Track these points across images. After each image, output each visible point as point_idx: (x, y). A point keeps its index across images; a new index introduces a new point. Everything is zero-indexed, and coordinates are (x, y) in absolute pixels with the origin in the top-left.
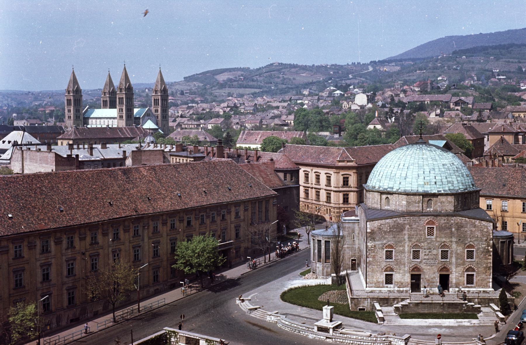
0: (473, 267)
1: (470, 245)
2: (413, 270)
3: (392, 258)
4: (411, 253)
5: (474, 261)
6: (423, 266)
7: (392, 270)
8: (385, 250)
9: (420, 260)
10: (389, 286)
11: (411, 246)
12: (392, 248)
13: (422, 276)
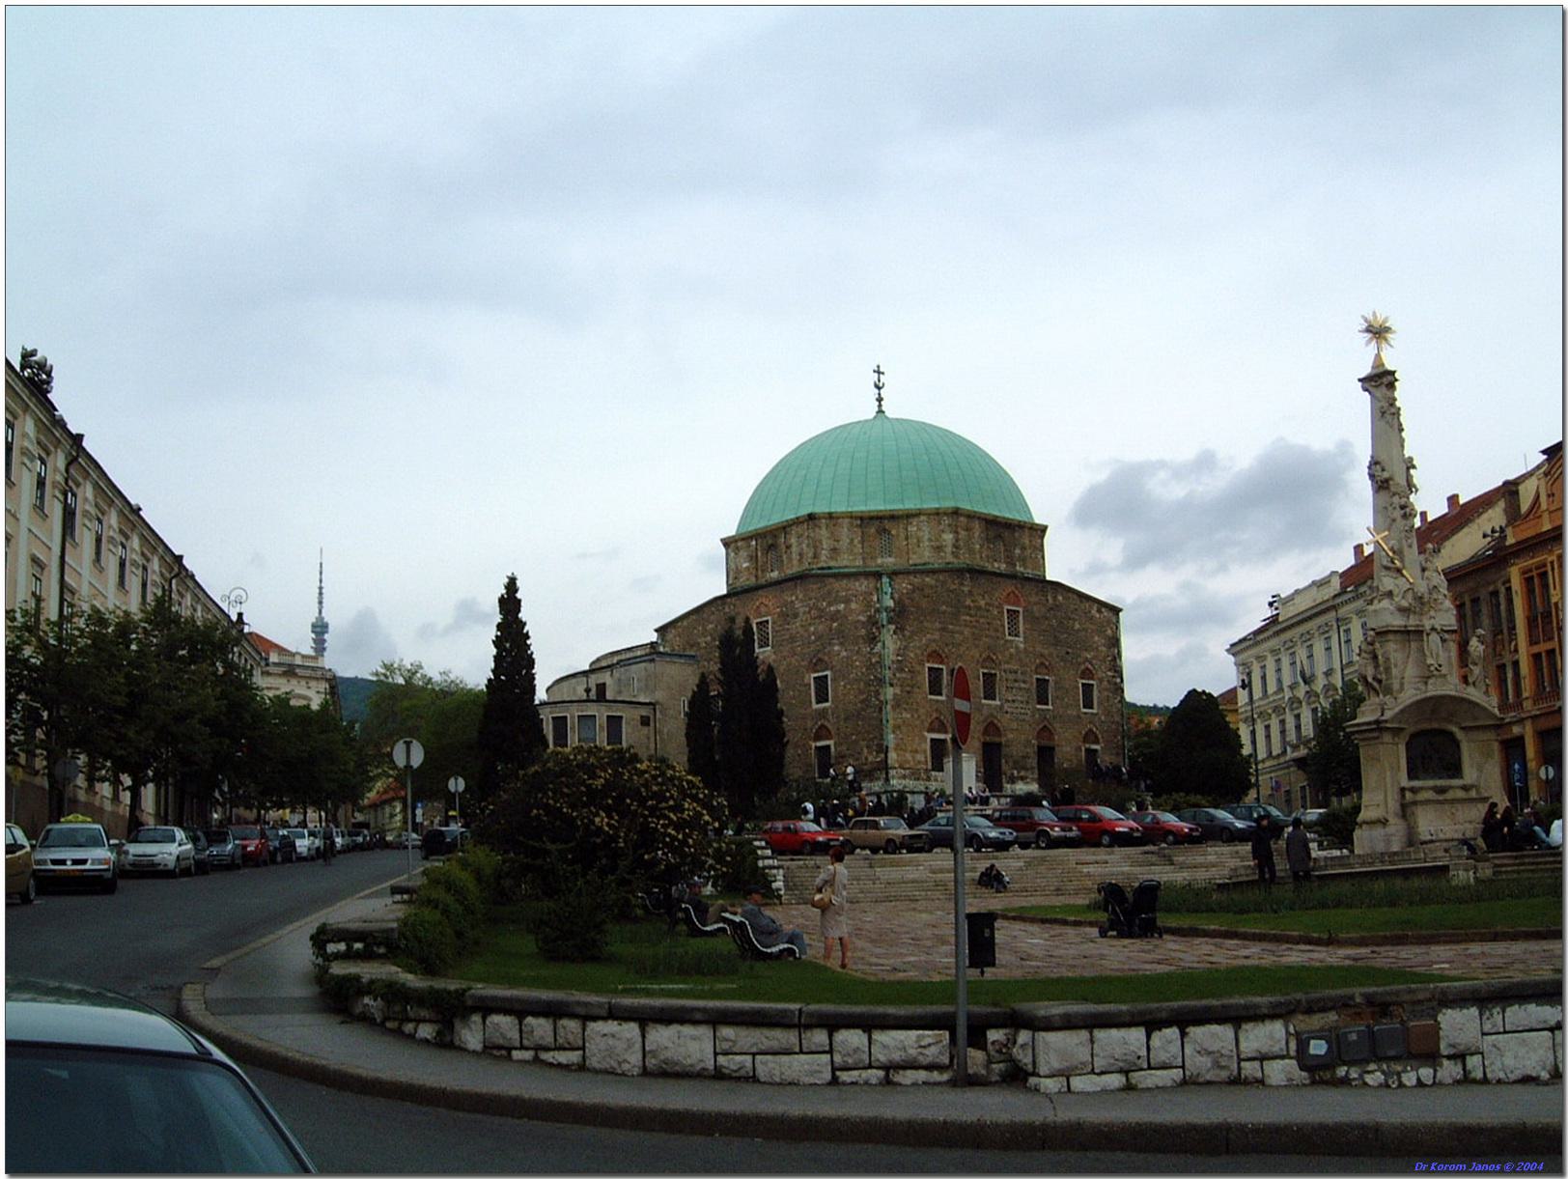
1: (1087, 669)
2: (986, 732)
5: (1097, 714)
6: (1004, 721)
8: (928, 665)
9: (998, 703)
12: (941, 663)
13: (1005, 751)
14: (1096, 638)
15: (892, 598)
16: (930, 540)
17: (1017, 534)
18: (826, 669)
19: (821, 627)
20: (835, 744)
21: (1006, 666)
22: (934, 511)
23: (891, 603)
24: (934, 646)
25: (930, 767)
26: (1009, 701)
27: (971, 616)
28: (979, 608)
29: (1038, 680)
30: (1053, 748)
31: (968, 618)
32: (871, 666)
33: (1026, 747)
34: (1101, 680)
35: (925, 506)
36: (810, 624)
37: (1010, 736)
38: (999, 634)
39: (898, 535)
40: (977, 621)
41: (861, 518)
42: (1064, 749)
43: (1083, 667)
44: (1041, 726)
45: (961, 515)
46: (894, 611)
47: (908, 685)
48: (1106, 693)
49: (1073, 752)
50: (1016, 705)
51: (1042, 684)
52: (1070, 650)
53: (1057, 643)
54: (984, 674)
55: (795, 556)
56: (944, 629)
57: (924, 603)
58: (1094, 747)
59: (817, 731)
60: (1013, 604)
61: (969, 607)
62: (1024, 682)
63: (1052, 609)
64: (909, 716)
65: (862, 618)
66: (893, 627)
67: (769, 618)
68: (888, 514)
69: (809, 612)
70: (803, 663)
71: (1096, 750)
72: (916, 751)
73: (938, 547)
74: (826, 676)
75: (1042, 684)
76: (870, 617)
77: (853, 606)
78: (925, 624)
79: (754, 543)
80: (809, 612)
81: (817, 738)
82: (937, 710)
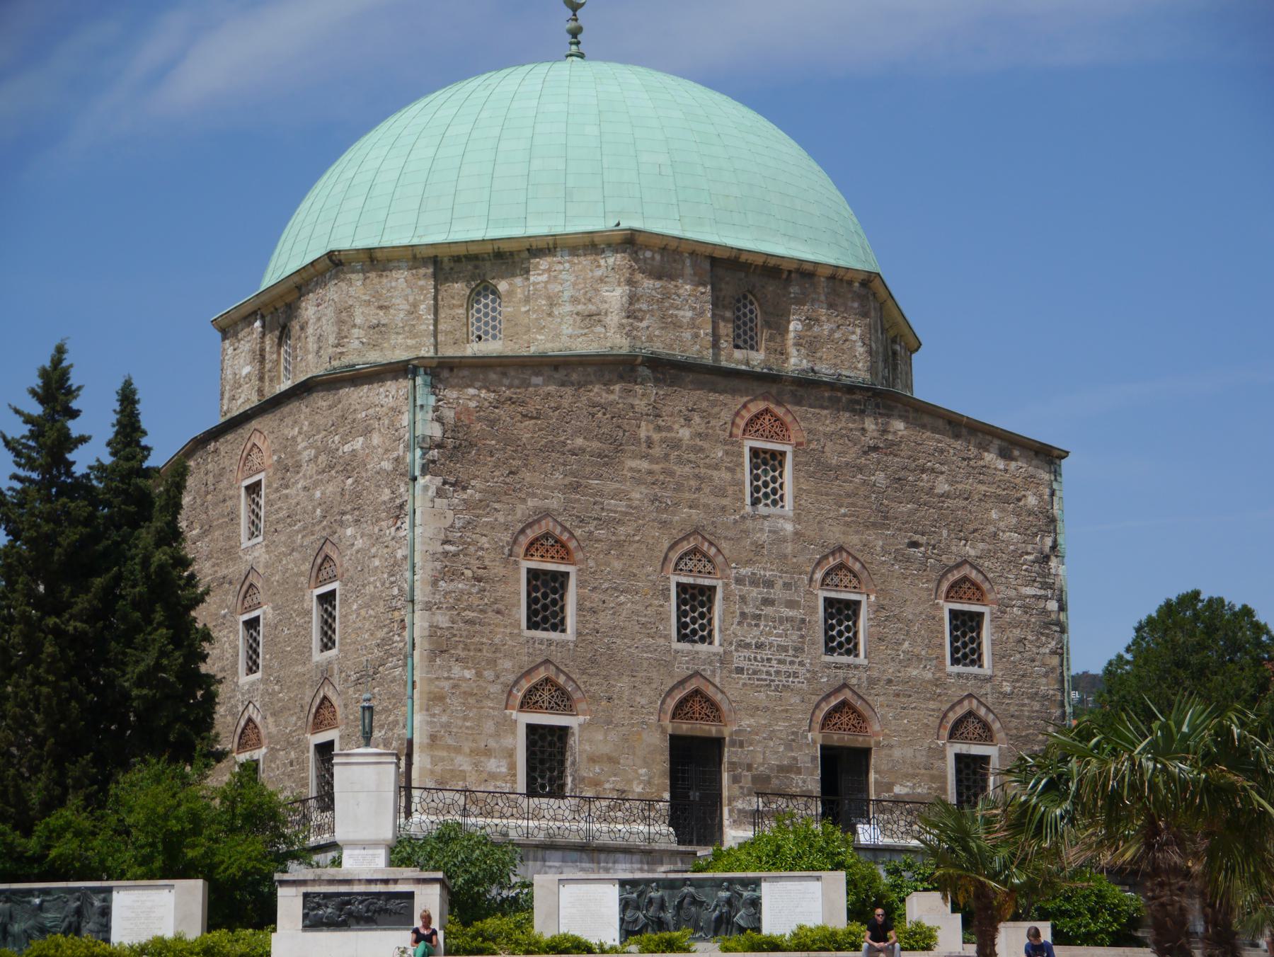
0: (982, 711)
2: (680, 711)
3: (559, 626)
4: (667, 598)
5: (989, 679)
7: (563, 702)
8: (526, 564)
10: (545, 804)
11: (666, 558)
14: (994, 515)
15: (439, 419)
16: (574, 300)
17: (794, 290)
18: (332, 579)
19: (330, 488)
20: (341, 737)
21: (743, 571)
22: (587, 240)
23: (436, 431)
24: (547, 525)
25: (521, 786)
26: (748, 646)
27: (653, 460)
28: (676, 444)
29: (829, 602)
30: (865, 753)
31: (644, 465)
32: (394, 567)
33: (789, 747)
34: (1004, 605)
35: (570, 229)
36: (316, 484)
37: (747, 722)
38: (725, 502)
39: (511, 293)
40: (671, 474)
41: (435, 261)
42: (897, 753)
43: (956, 575)
44: (834, 702)
45: (647, 247)
46: (439, 446)
47: (470, 608)
48: (1017, 632)
49: (921, 759)
50: (766, 653)
51: (841, 611)
52: (923, 540)
53: (883, 519)
54: (682, 588)
55: (312, 346)
56: (575, 487)
57: (526, 431)
58: (977, 750)
59: (317, 711)
60: (769, 438)
61: (650, 444)
62: (791, 604)
63: (875, 449)
64: (468, 674)
65: (387, 465)
66: (439, 481)
67: (261, 476)
68: (489, 248)
69: (316, 457)
70: (303, 568)
71: (985, 759)
72: (488, 752)
73: (590, 316)
74: (334, 591)
75: (841, 611)
76: (397, 460)
77: (376, 439)
78: (527, 476)
79: (258, 324)
80: (316, 457)
81: (318, 726)
82: (547, 662)
